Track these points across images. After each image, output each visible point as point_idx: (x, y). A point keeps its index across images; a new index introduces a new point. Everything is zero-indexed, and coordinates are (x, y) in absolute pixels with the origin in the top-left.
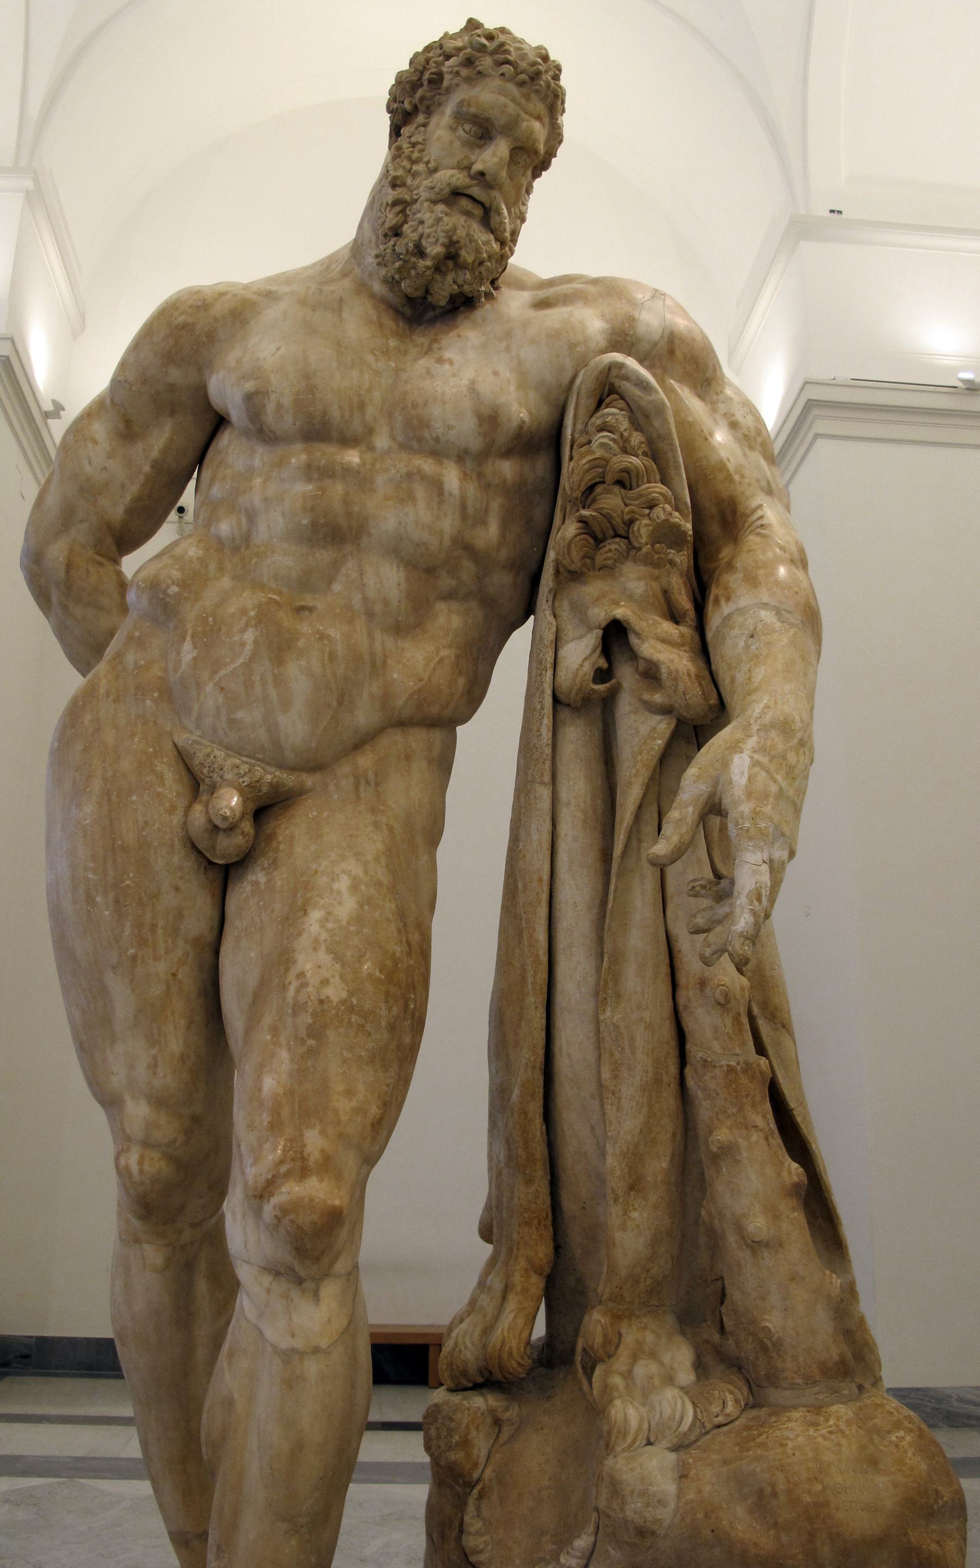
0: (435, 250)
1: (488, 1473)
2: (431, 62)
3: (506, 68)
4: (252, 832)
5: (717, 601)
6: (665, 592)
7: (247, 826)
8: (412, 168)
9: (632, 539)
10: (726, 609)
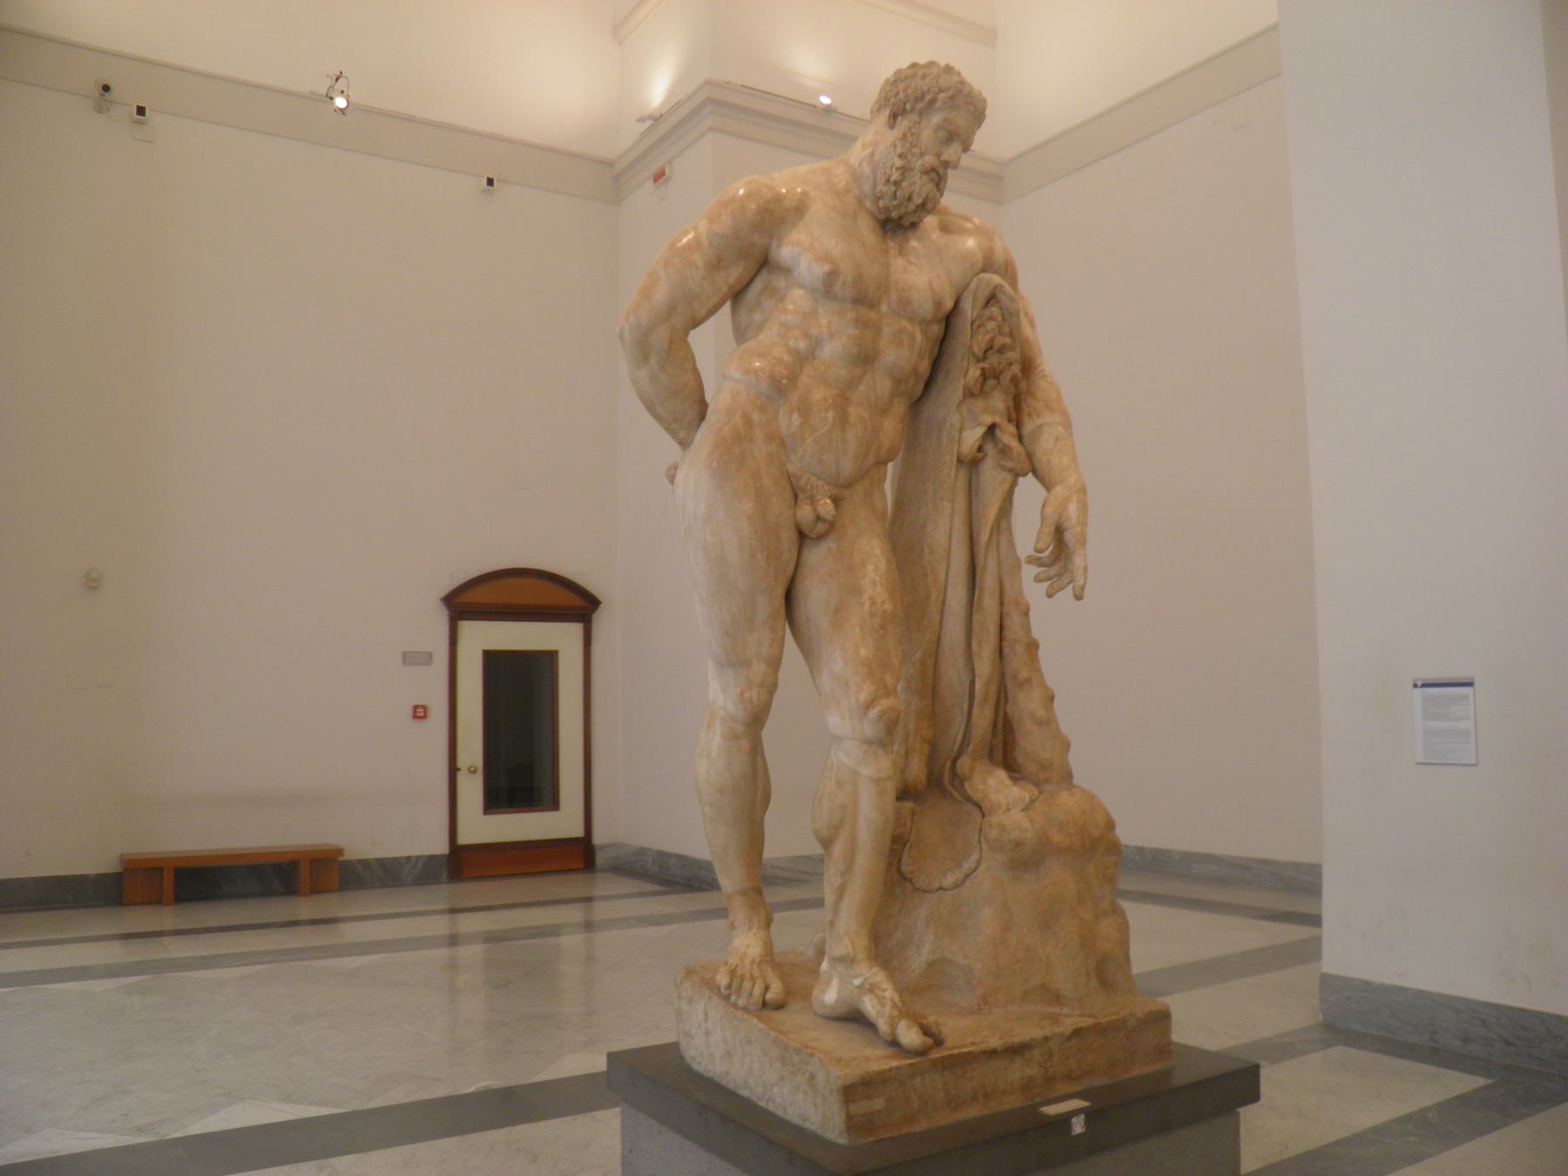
0: (918, 201)
1: (912, 838)
2: (932, 89)
3: (971, 108)
5: (1030, 415)
6: (1008, 408)
8: (911, 150)
9: (1001, 379)
10: (1038, 422)
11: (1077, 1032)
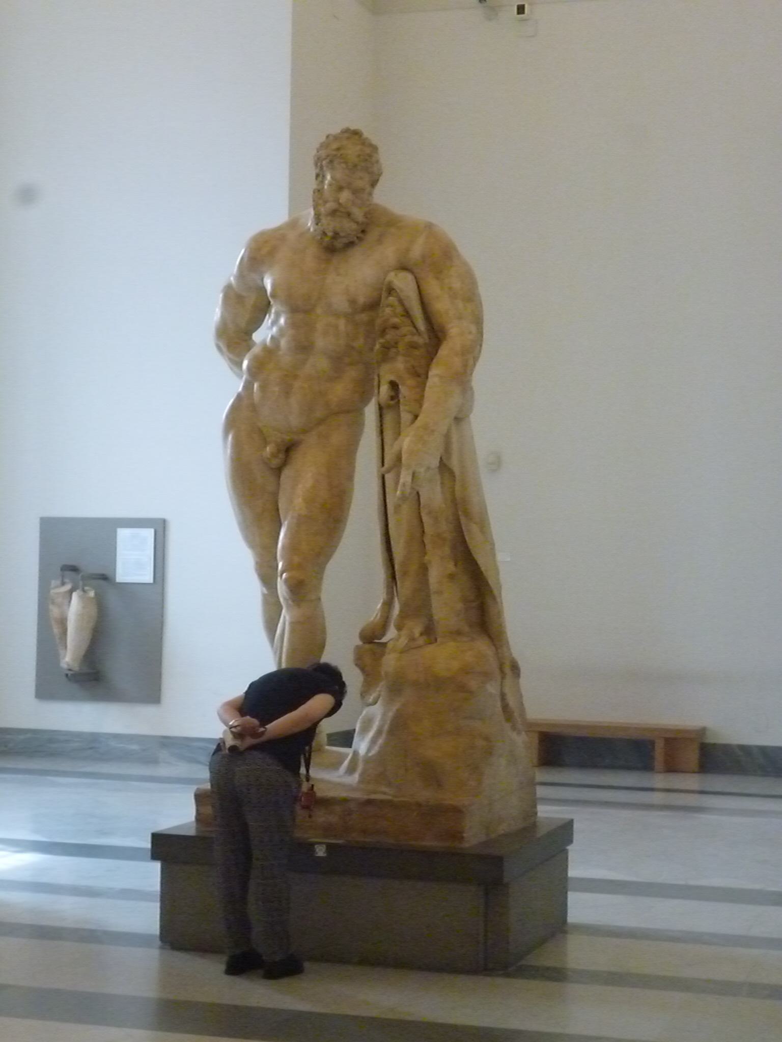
0: (330, 234)
4: (284, 457)
6: (413, 367)
7: (282, 456)
11: (369, 802)
